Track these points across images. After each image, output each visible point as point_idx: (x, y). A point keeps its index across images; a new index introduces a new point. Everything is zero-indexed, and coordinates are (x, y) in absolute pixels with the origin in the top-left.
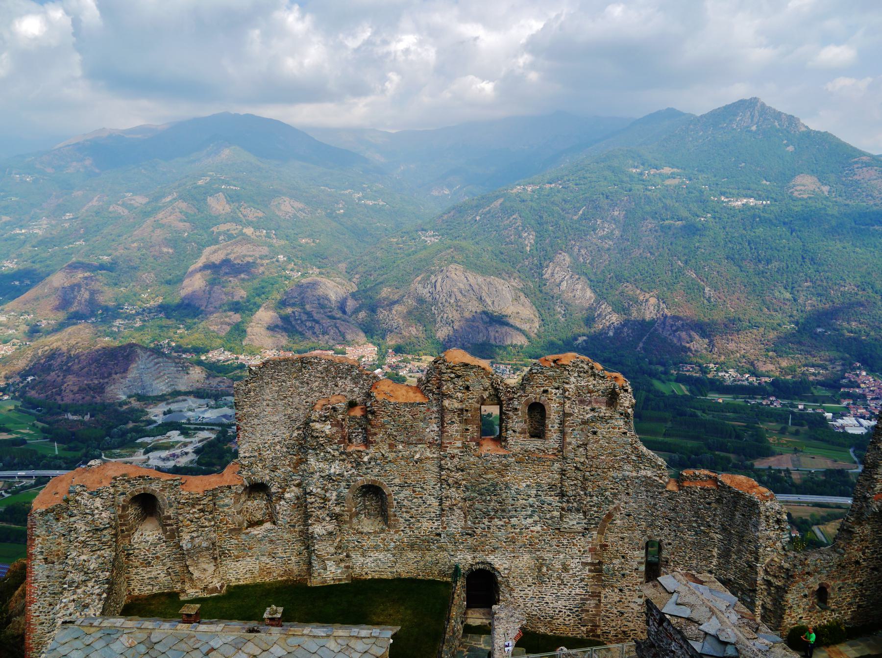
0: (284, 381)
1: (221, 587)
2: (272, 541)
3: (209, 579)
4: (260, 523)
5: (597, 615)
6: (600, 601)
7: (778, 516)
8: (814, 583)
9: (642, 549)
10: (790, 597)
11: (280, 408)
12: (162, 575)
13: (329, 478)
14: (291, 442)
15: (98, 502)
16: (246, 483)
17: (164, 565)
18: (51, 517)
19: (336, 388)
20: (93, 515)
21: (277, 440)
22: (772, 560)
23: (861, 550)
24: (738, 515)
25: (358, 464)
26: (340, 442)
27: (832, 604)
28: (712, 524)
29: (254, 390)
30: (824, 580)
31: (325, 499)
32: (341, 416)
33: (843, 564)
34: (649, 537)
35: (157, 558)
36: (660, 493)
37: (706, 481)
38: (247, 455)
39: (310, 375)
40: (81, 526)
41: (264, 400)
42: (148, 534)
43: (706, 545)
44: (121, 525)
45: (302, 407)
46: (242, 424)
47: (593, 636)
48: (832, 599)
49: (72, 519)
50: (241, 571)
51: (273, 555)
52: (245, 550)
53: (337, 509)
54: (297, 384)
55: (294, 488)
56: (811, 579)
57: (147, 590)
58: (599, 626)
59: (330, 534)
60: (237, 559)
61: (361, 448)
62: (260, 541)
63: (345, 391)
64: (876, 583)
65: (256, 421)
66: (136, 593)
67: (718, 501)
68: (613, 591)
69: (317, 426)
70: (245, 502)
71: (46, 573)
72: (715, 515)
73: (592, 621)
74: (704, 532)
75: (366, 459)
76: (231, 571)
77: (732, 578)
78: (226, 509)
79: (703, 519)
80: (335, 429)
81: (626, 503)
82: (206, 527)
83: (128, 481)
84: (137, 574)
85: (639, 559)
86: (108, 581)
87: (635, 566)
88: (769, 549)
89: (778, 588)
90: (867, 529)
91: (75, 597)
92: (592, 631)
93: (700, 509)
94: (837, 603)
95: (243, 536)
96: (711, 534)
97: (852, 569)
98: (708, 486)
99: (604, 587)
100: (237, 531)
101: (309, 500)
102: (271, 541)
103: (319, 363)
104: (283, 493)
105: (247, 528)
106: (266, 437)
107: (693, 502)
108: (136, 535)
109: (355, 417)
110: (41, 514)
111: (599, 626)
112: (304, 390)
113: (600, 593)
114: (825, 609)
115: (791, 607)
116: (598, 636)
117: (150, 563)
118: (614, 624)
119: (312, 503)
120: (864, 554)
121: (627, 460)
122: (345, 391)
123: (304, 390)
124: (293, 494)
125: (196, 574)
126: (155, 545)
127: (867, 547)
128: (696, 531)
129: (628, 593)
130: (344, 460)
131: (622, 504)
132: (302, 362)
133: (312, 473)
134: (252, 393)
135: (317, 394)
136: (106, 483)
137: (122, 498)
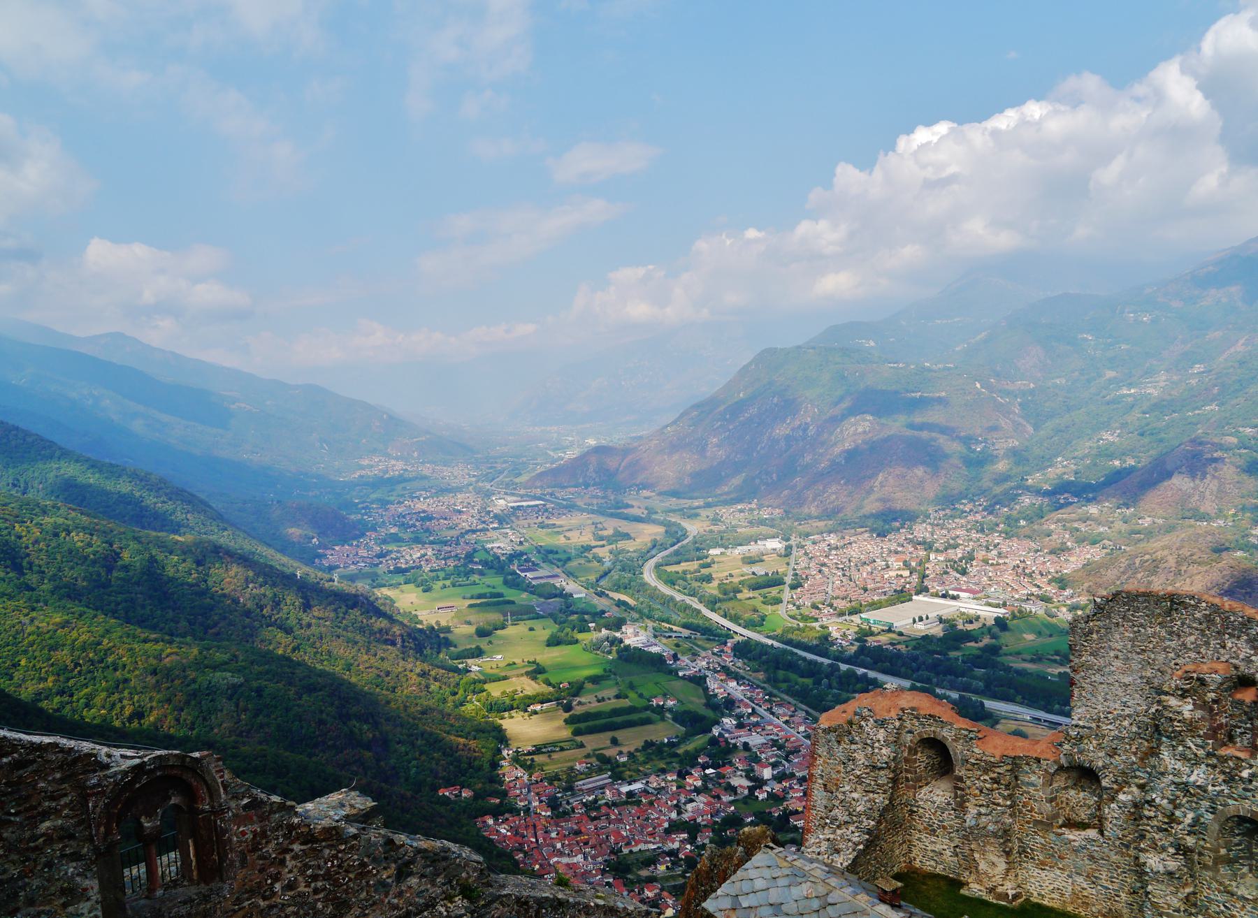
0: (1141, 625)
1: (1016, 897)
2: (1093, 857)
3: (998, 879)
4: (1083, 826)
11: (1135, 666)
12: (948, 853)
13: (1184, 787)
14: (1146, 719)
15: (881, 734)
16: (1063, 761)
17: (951, 839)
18: (832, 736)
19: (1222, 651)
20: (873, 748)
21: (1127, 711)
25: (1231, 779)
26: (1206, 736)
29: (1098, 632)
31: (1172, 819)
32: (1212, 695)
38: (1081, 723)
39: (1183, 624)
40: (860, 757)
42: (936, 795)
44: (907, 771)
45: (1169, 671)
46: (1077, 677)
49: (853, 747)
51: (1093, 879)
52: (1051, 859)
53: (1190, 841)
54: (1163, 633)
55: (1135, 789)
57: (929, 866)
59: (1170, 874)
60: (1042, 865)
61: (1242, 755)
62: (1076, 851)
63: (1237, 657)
65: (1098, 678)
66: (917, 864)
69: (1173, 702)
70: (1066, 788)
71: (824, 802)
75: (1245, 774)
76: (1032, 880)
78: (1031, 789)
80: (1199, 714)
82: (998, 805)
84: (919, 839)
86: (869, 832)
91: (832, 836)
100: (1045, 825)
101: (1146, 813)
102: (1092, 858)
103: (1196, 607)
104: (1117, 792)
105: (1061, 827)
106: (1112, 705)
108: (924, 790)
109: (1241, 702)
110: (824, 730)
112: (1173, 644)
117: (934, 831)
119: (1149, 818)
122: (1237, 657)
123: (1173, 644)
124: (1130, 797)
125: (983, 866)
126: (943, 810)
130: (1214, 767)
132: (1172, 601)
133: (1163, 774)
134: (1095, 636)
135: (1193, 655)
136: (893, 714)
137: (909, 737)
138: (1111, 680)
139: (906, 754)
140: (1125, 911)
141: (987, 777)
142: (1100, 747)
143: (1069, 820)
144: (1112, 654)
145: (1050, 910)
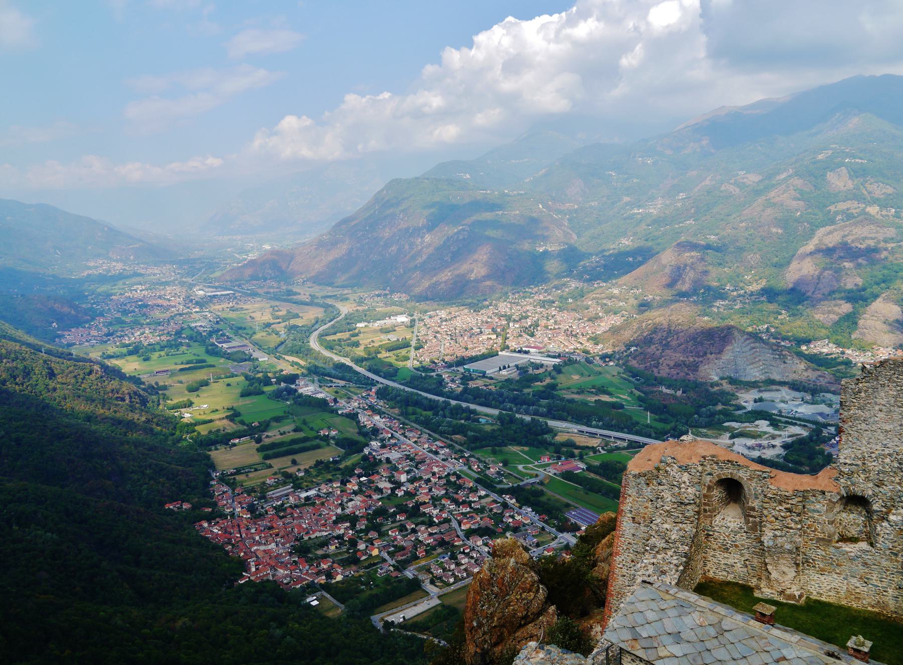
1: (801, 596)
2: (866, 564)
3: (787, 584)
4: (854, 540)
12: (739, 565)
15: (686, 477)
16: (843, 492)
17: (742, 555)
18: (642, 480)
21: (887, 451)
29: (866, 391)
35: (736, 546)
38: (848, 461)
40: (668, 496)
41: (876, 403)
42: (729, 519)
44: (705, 504)
46: (846, 426)
49: (661, 488)
50: (825, 586)
51: (866, 581)
52: (832, 565)
57: (721, 576)
60: (822, 572)
62: (852, 560)
66: (711, 575)
70: (839, 512)
71: (632, 531)
76: (813, 583)
78: (816, 515)
82: (791, 528)
83: (717, 463)
84: (714, 556)
86: (686, 555)
91: (655, 561)
95: (832, 550)
100: (826, 541)
102: (865, 564)
104: (887, 513)
105: (837, 542)
106: (874, 446)
108: (718, 518)
110: (635, 476)
117: (728, 549)
125: (774, 575)
126: (736, 533)
134: (863, 394)
136: (695, 460)
137: (709, 478)
138: (874, 428)
139: (705, 492)
140: (891, 602)
141: (781, 508)
142: (867, 479)
143: (842, 536)
144: (877, 408)
145: (829, 605)
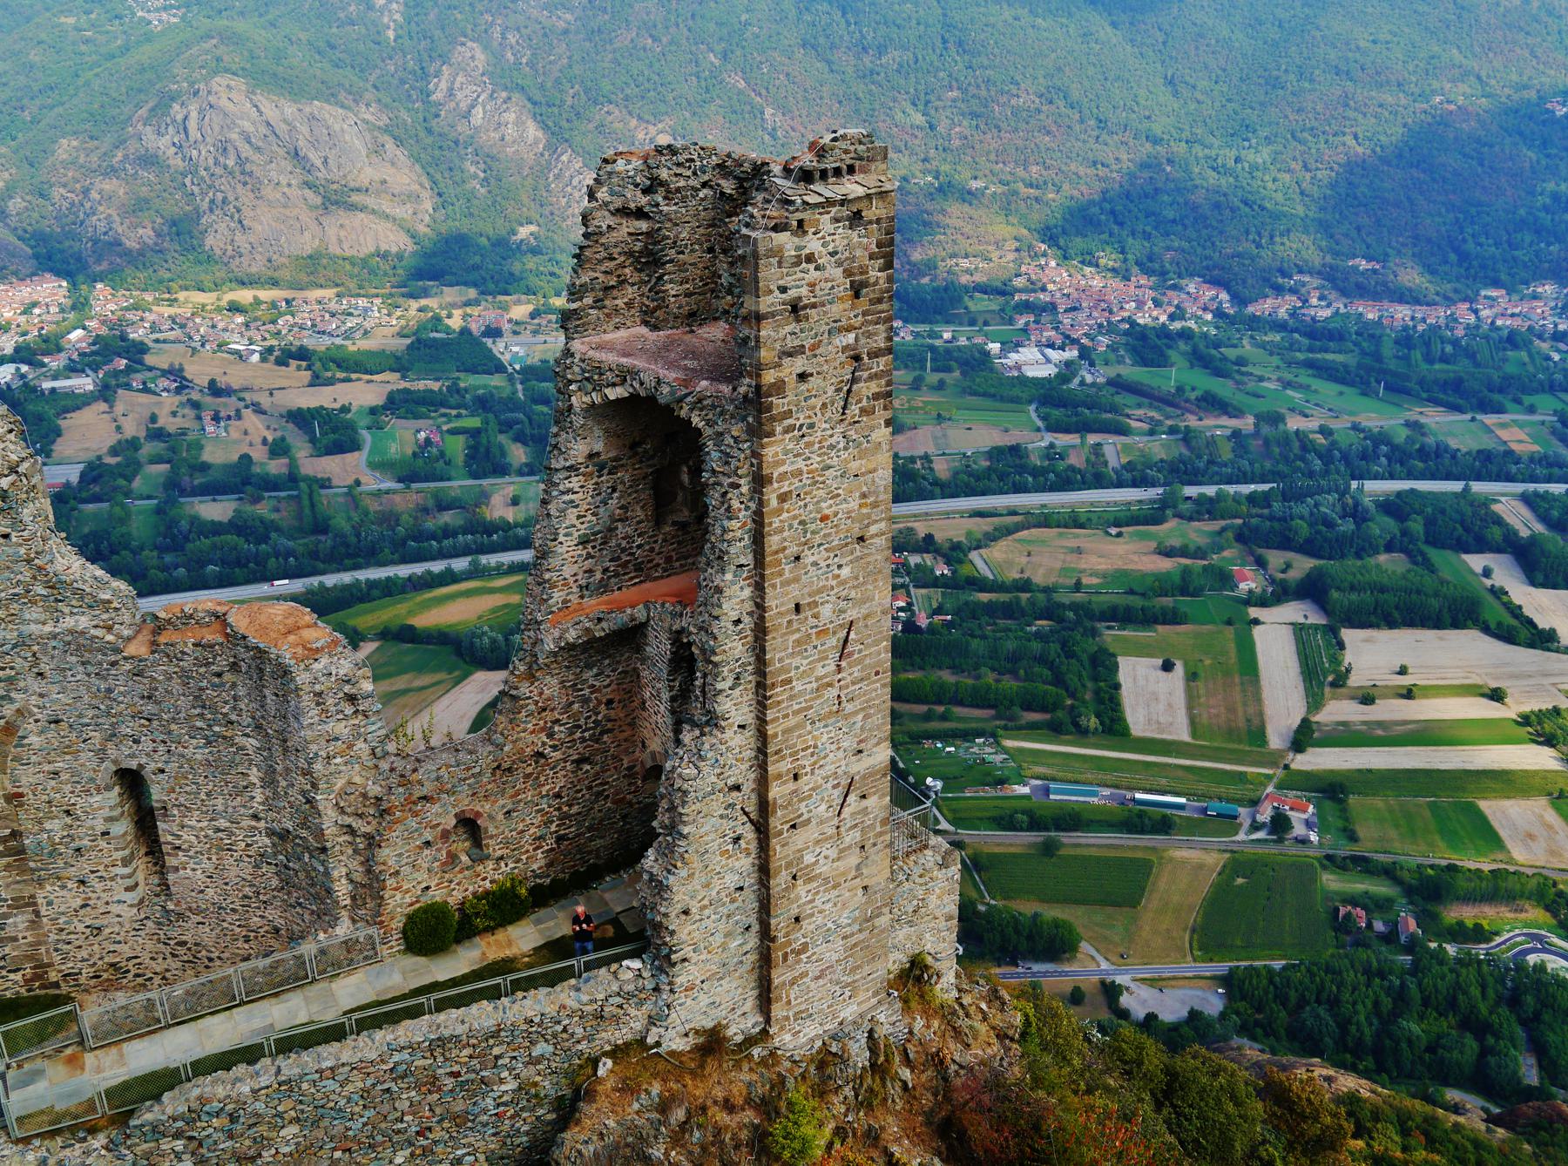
5: (39, 943)
6: (37, 913)
7: (347, 689)
8: (443, 815)
9: (108, 788)
10: (387, 855)
22: (350, 783)
23: (542, 729)
24: (270, 698)
27: (494, 847)
28: (234, 717)
30: (465, 804)
33: (505, 766)
34: (115, 762)
36: (113, 664)
37: (208, 625)
43: (232, 764)
47: (42, 987)
48: (491, 837)
56: (436, 808)
58: (50, 965)
64: (589, 788)
67: (234, 667)
68: (63, 887)
72: (235, 698)
73: (30, 958)
74: (225, 738)
77: (289, 825)
79: (214, 709)
81: (41, 695)
85: (106, 813)
87: (100, 828)
88: (338, 760)
89: (369, 837)
90: (551, 686)
92: (36, 977)
93: (201, 689)
94: (506, 843)
96: (237, 740)
97: (529, 770)
98: (210, 636)
99: (40, 883)
107: (185, 676)
111: (50, 965)
113: (33, 896)
114: (482, 860)
115: (397, 873)
116: (56, 985)
118: (84, 954)
120: (551, 735)
121: (25, 596)
127: (557, 721)
128: (205, 737)
129: (99, 886)
131: (34, 700)
